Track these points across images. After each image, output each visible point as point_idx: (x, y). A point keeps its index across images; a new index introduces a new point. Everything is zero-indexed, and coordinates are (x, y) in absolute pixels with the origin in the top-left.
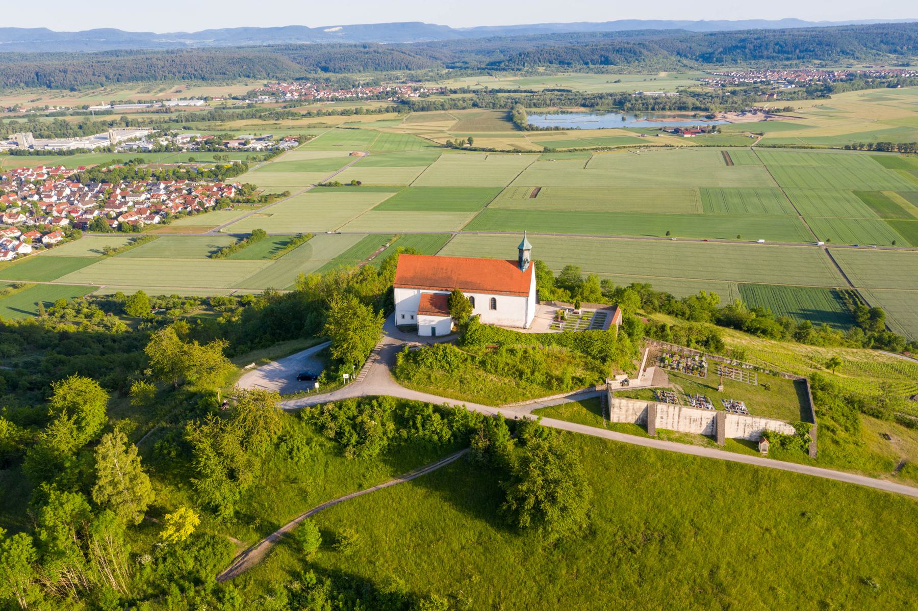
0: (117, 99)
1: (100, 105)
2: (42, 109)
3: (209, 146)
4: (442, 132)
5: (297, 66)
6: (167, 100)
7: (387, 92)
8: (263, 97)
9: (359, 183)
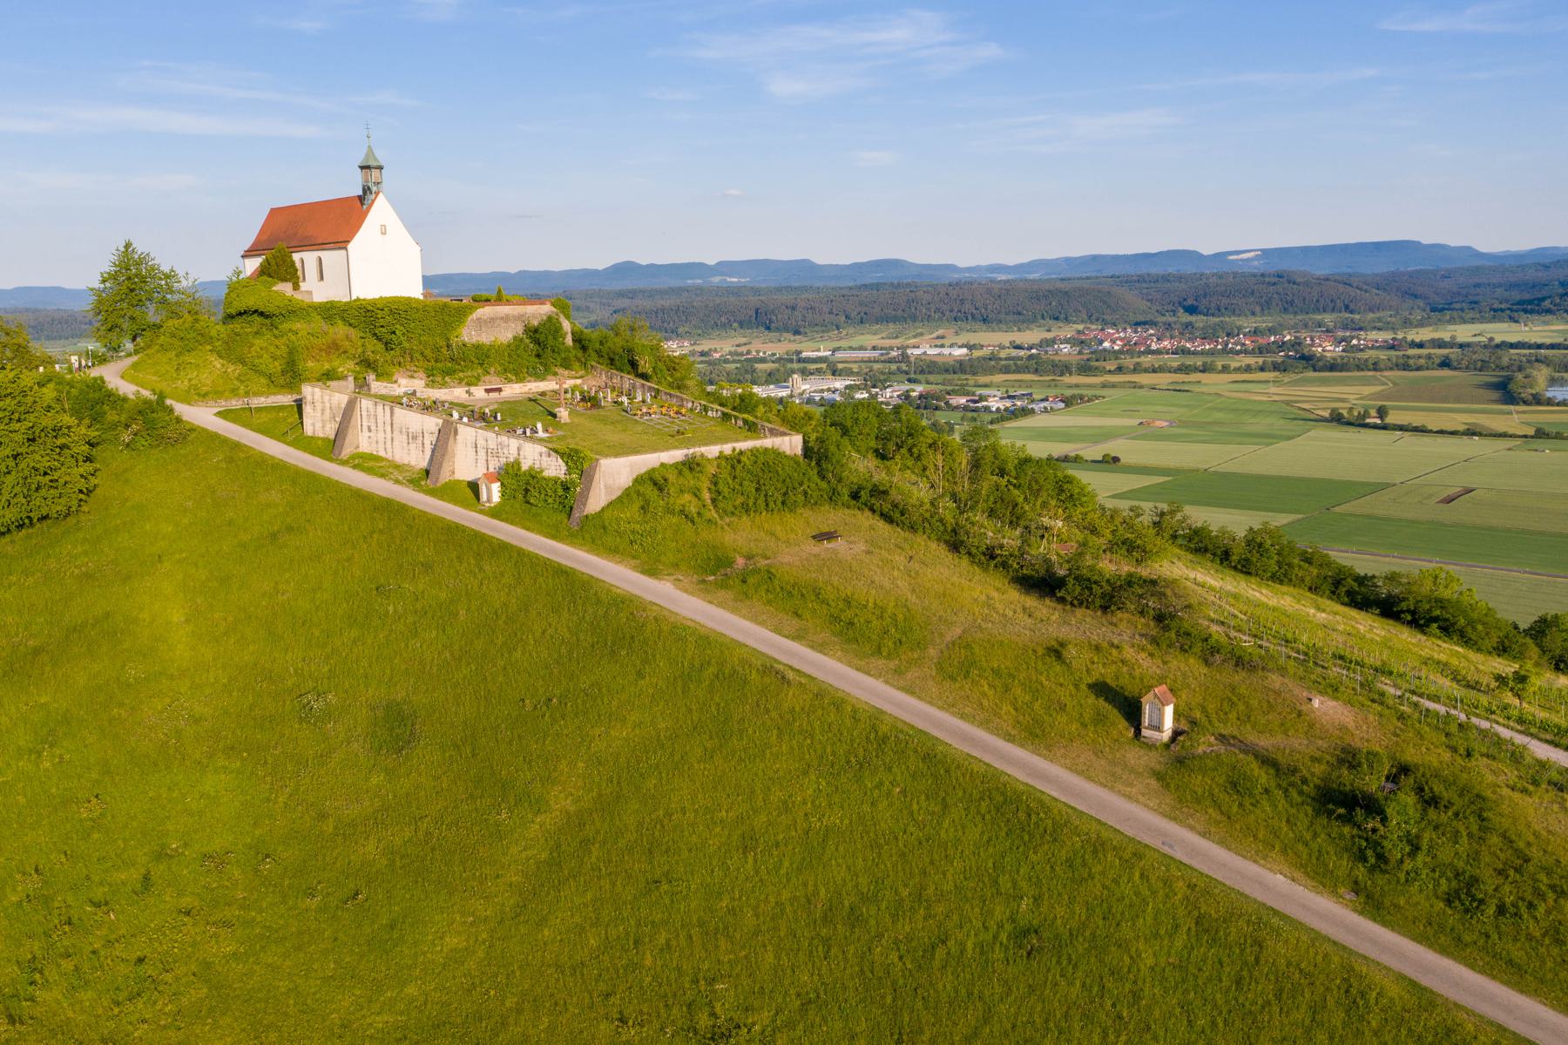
0: (843, 343)
1: (819, 350)
2: (742, 354)
4: (1343, 400)
5: (1144, 305)
6: (914, 347)
7: (1284, 343)
8: (1062, 346)
9: (1116, 459)
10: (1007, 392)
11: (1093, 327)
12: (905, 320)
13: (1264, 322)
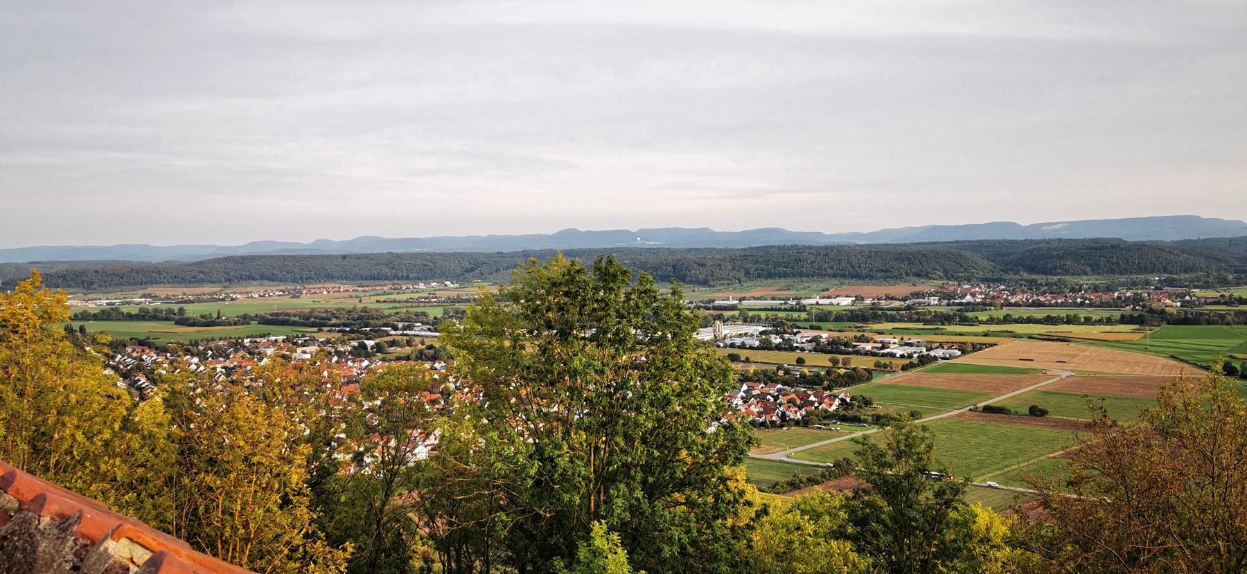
3: (833, 347)
10: (902, 339)
11: (951, 283)
12: (794, 276)
13: (1101, 281)
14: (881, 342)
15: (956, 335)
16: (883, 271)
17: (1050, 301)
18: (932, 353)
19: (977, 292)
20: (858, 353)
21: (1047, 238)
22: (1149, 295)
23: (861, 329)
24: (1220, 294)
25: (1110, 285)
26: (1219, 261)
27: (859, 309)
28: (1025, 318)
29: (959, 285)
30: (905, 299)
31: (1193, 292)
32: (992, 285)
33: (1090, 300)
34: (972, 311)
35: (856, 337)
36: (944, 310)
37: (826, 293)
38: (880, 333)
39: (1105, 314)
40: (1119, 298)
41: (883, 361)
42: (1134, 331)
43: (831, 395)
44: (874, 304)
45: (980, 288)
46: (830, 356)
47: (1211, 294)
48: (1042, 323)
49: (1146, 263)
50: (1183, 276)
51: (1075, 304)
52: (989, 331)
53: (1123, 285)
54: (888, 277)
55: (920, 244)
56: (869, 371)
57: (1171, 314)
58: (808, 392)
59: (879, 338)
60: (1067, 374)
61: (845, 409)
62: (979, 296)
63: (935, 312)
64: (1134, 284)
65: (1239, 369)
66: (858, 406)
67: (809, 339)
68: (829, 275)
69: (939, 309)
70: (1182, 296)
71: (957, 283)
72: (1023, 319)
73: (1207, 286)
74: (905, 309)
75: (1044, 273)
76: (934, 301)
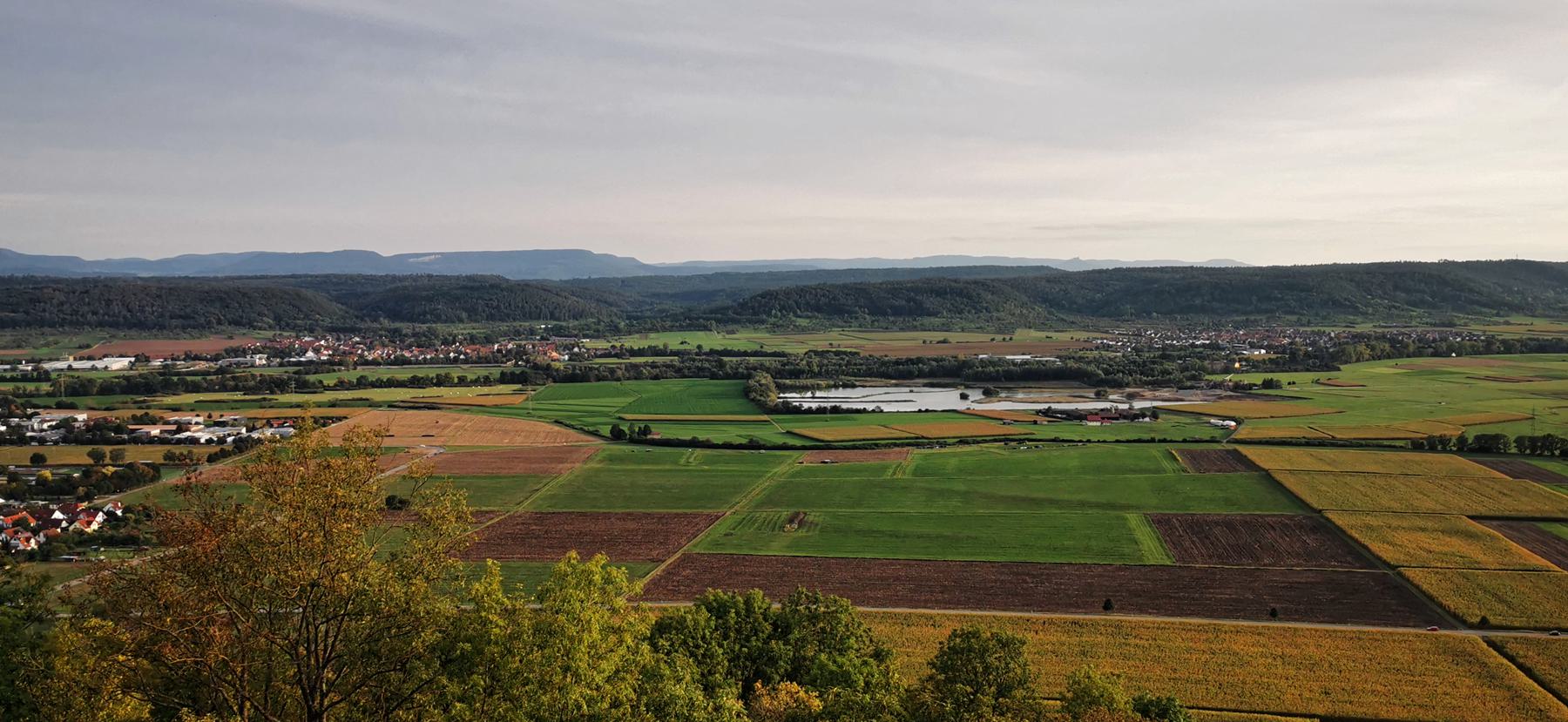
3: (95, 434)
10: (210, 416)
11: (285, 334)
13: (479, 329)
14: (176, 422)
15: (291, 407)
16: (181, 317)
17: (417, 357)
18: (255, 435)
19: (322, 345)
20: (136, 441)
21: (415, 274)
22: (534, 347)
23: (144, 405)
24: (611, 344)
25: (489, 335)
26: (611, 305)
27: (140, 375)
28: (385, 380)
29: (298, 337)
30: (216, 359)
31: (582, 342)
32: (342, 336)
33: (466, 354)
34: (315, 373)
35: (134, 417)
36: (276, 372)
37: (86, 352)
38: (175, 409)
39: (481, 372)
40: (499, 351)
41: (177, 450)
42: (515, 393)
43: (90, 508)
44: (165, 367)
45: (327, 340)
46: (89, 448)
47: (602, 344)
48: (406, 386)
49: (530, 307)
50: (572, 323)
51: (448, 361)
52: (337, 400)
53: (505, 335)
54: (189, 326)
55: (240, 278)
56: (155, 468)
57: (557, 370)
58: (51, 506)
59: (175, 417)
60: (435, 451)
61: (115, 528)
62: (326, 352)
63: (261, 375)
64: (518, 333)
65: (627, 432)
66: (136, 521)
67: (54, 423)
68: (90, 324)
69: (268, 372)
70: (569, 348)
71: (294, 334)
72: (382, 381)
73: (597, 335)
74: (215, 373)
75: (411, 320)
76: (260, 360)
